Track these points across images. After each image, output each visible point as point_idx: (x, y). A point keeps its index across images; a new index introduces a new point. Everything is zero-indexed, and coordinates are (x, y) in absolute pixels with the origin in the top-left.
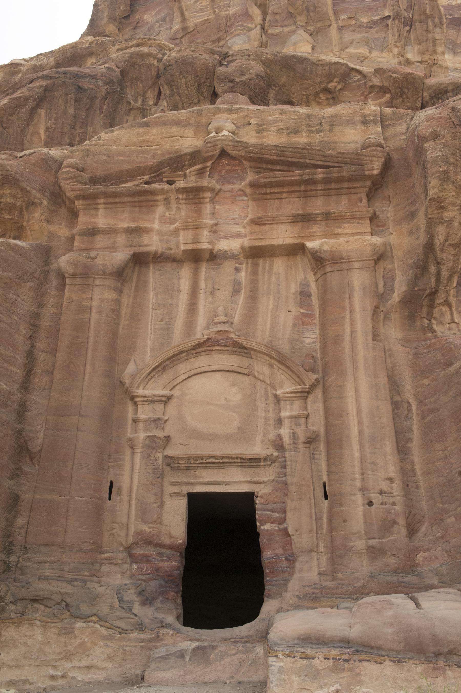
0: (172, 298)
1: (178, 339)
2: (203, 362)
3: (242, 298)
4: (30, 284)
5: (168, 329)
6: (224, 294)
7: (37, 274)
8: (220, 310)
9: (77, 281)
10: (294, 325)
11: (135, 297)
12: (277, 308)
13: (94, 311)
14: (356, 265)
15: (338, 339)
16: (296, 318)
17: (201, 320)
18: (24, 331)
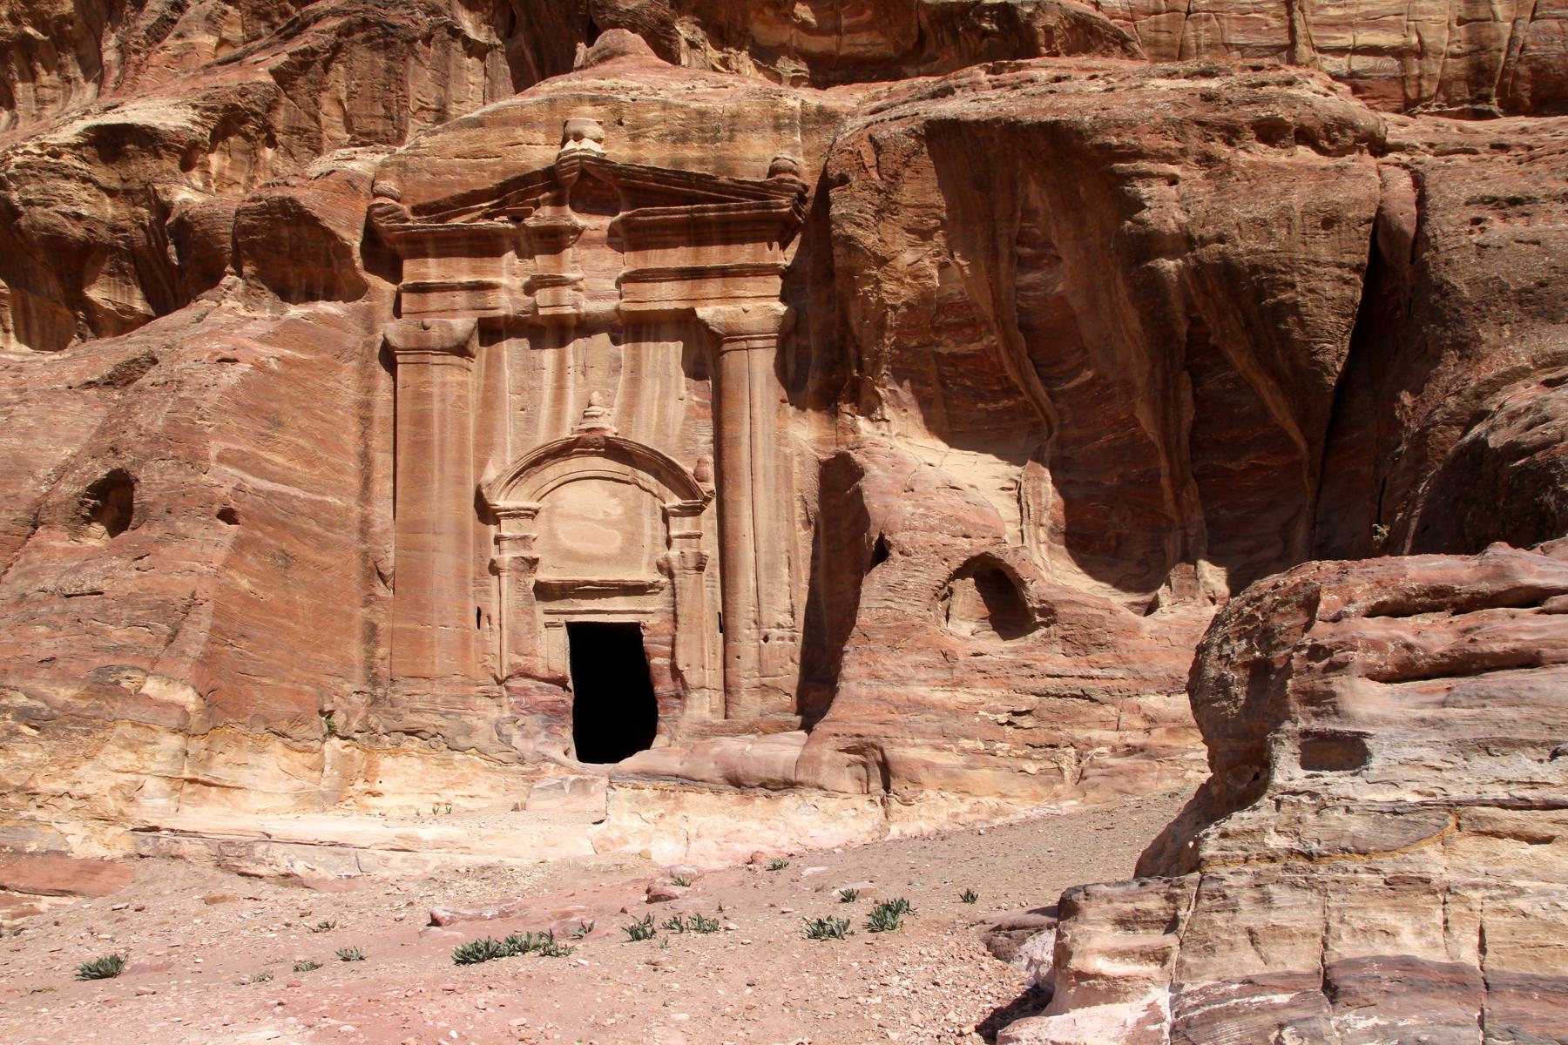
0: (533, 378)
1: (543, 437)
2: (574, 465)
3: (621, 380)
4: (353, 364)
5: (530, 421)
6: (597, 375)
7: (359, 349)
8: (596, 396)
9: (410, 358)
10: (686, 418)
11: (487, 377)
12: (664, 395)
13: (436, 399)
14: (759, 343)
15: (736, 441)
16: (690, 409)
17: (572, 410)
18: (354, 428)
